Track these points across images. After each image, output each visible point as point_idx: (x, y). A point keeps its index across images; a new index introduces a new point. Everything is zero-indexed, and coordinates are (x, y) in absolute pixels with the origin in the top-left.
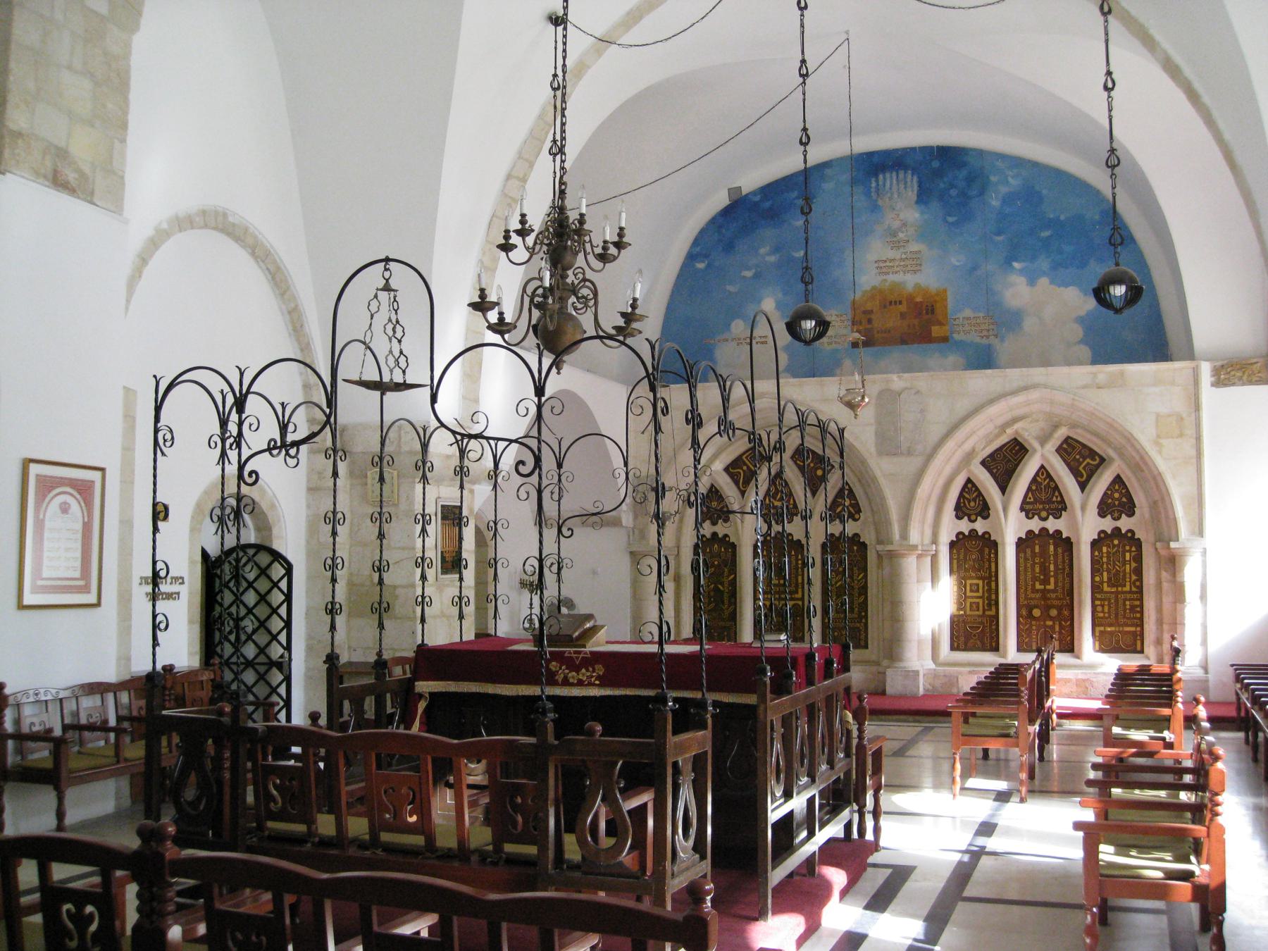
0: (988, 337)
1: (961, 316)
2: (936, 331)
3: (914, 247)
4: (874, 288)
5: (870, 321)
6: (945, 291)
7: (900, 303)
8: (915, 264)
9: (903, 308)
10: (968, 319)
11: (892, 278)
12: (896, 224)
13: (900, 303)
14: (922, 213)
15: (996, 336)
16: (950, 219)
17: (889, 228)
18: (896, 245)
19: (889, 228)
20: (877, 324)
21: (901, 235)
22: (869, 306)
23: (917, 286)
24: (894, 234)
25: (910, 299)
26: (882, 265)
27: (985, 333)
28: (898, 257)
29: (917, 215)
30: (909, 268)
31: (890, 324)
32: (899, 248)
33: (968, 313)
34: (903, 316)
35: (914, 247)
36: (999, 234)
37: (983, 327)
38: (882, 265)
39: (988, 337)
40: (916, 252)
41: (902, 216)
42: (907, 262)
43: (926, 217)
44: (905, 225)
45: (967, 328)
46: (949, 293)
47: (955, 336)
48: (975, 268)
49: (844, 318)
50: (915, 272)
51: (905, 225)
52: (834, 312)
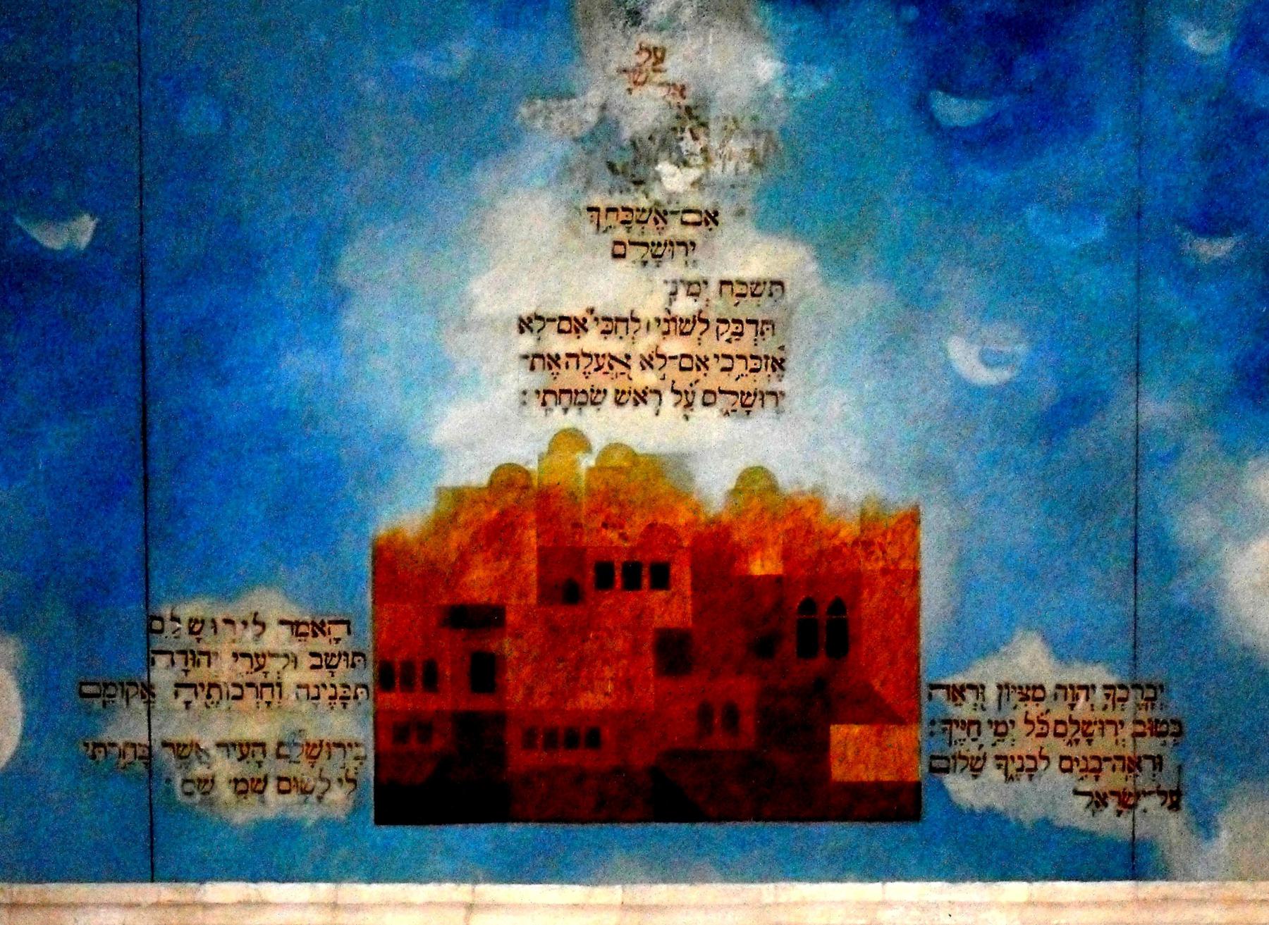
0: (1127, 801)
1: (989, 673)
2: (853, 750)
3: (749, 255)
4: (509, 479)
5: (485, 672)
6: (913, 519)
7: (661, 577)
8: (745, 355)
9: (670, 608)
10: (1032, 692)
11: (607, 426)
12: (647, 109)
13: (661, 577)
14: (796, 56)
15: (1173, 799)
16: (956, 111)
17: (606, 125)
18: (645, 234)
19: (606, 125)
20: (522, 687)
21: (673, 180)
22: (479, 580)
23: (755, 481)
24: (632, 166)
25: (716, 548)
26: (559, 345)
27: (1113, 779)
28: (650, 308)
29: (767, 68)
30: (714, 378)
31: (592, 700)
32: (656, 253)
33: (1030, 660)
34: (674, 651)
35: (749, 255)
36: (1209, 226)
37: (1104, 744)
38: (559, 345)
39: (1127, 801)
40: (755, 289)
41: (675, 68)
42: (712, 345)
43: (819, 80)
44: (691, 114)
45: (1023, 743)
46: (926, 539)
47: (960, 786)
48: (1070, 411)
49: (335, 640)
50: (745, 403)
51: (691, 114)
52: (273, 605)
